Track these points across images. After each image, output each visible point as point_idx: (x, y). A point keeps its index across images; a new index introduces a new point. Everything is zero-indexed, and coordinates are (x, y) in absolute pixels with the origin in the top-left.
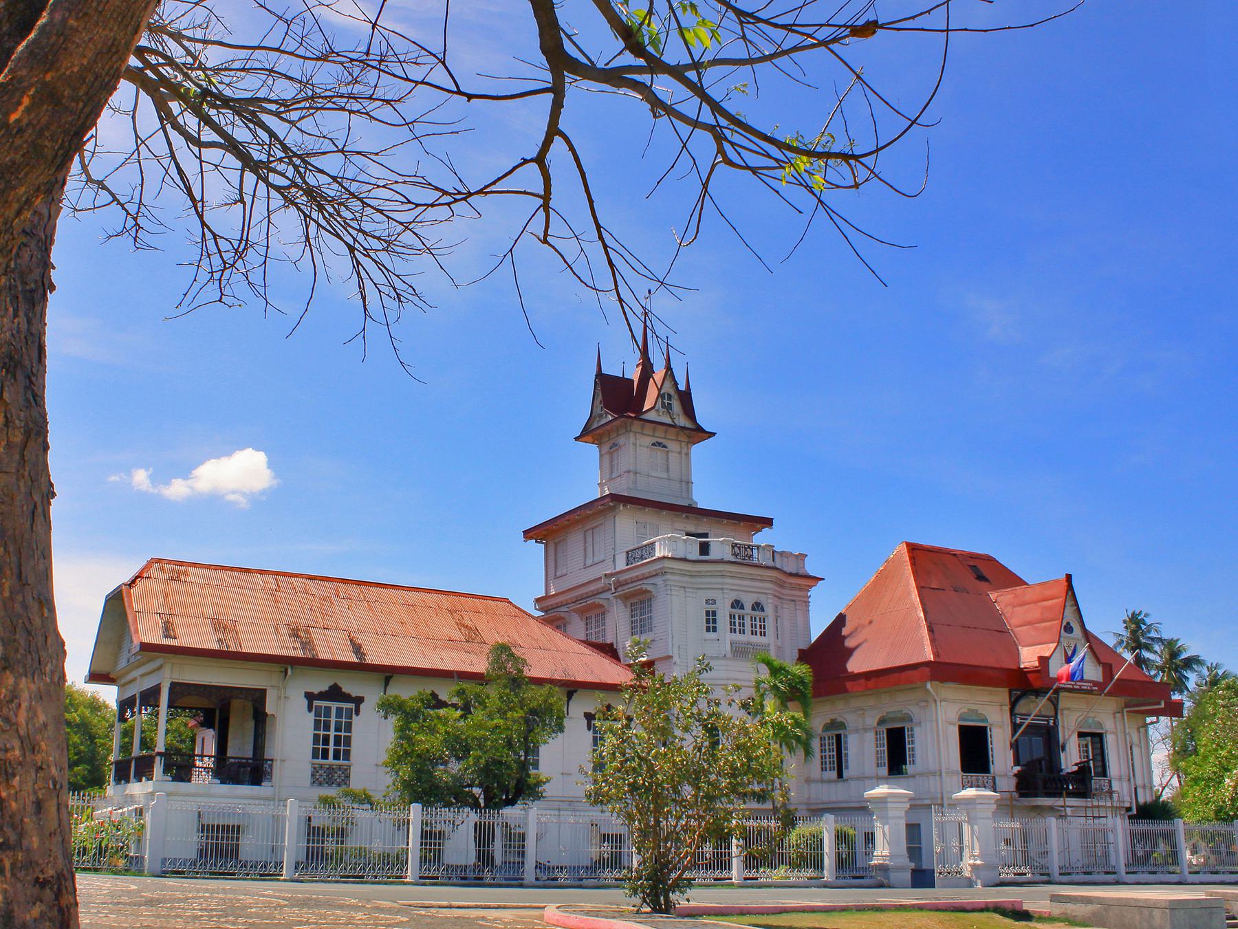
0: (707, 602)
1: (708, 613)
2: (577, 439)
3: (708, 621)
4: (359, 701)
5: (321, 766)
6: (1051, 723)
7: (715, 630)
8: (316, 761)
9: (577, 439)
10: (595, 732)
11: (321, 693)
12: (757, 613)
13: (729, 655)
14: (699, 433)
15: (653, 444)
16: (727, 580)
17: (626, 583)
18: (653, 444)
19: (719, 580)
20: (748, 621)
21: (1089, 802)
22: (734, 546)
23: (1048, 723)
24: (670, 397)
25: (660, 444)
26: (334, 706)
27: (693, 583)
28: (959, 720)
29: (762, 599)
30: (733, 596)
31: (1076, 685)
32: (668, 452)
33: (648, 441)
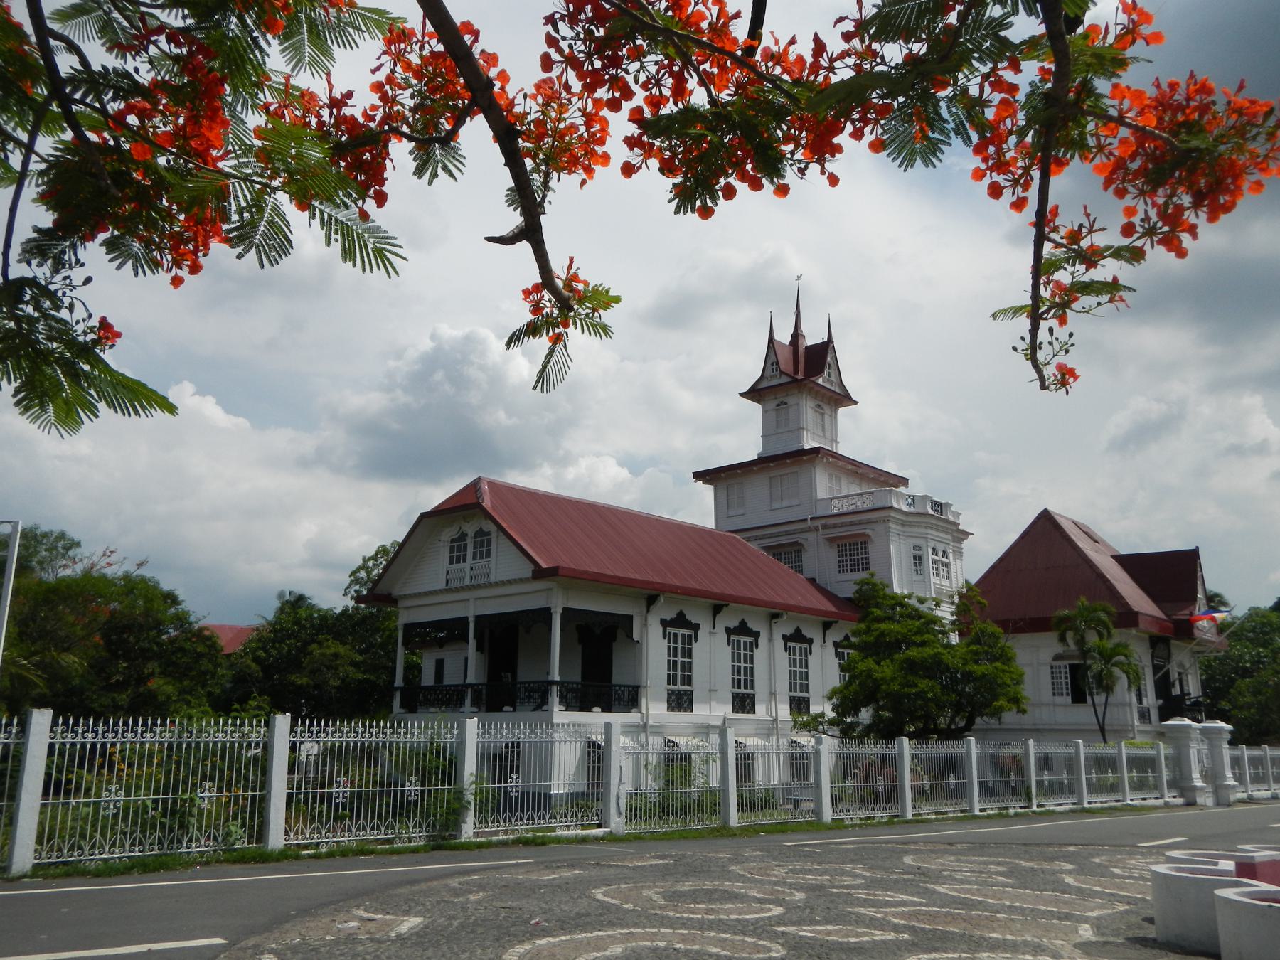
1: (915, 558)
2: (742, 395)
4: (696, 627)
5: (673, 691)
8: (672, 687)
9: (742, 395)
11: (672, 620)
12: (945, 560)
14: (844, 398)
16: (929, 531)
17: (834, 526)
19: (922, 530)
20: (941, 568)
25: (818, 406)
26: (680, 632)
30: (932, 544)
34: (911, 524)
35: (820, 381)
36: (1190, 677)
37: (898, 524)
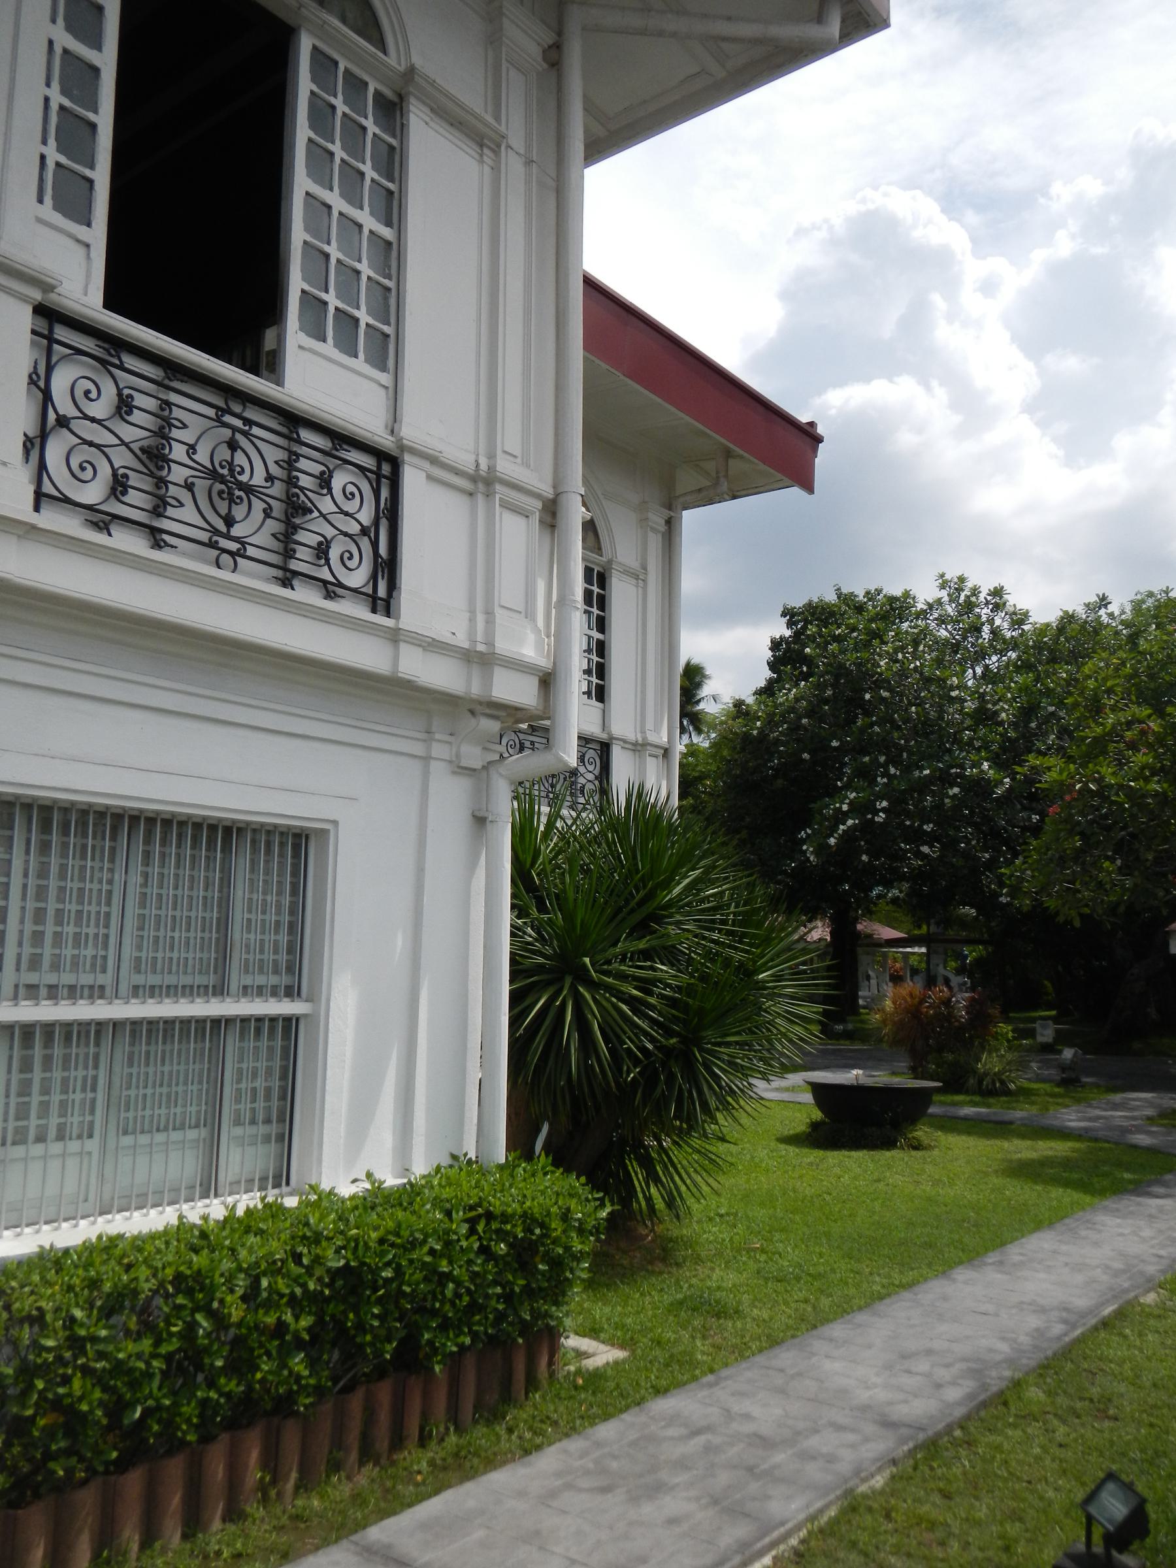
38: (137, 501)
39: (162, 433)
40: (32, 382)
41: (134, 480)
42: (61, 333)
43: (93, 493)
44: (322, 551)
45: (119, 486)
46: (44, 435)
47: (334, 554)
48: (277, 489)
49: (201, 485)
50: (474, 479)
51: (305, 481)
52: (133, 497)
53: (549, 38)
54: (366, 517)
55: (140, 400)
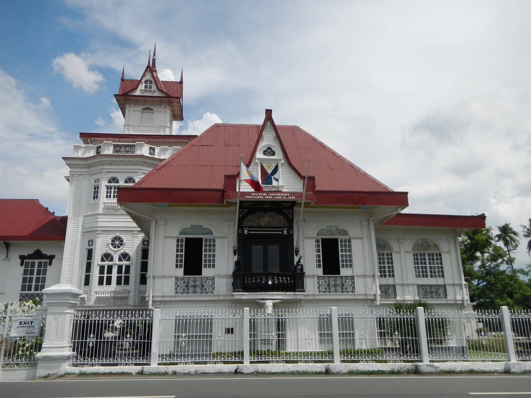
0: (95, 182)
1: (95, 188)
3: (95, 192)
6: (285, 232)
7: (97, 198)
10: (27, 265)
13: (100, 211)
15: (144, 109)
18: (144, 109)
19: (101, 167)
21: (299, 295)
22: (115, 146)
23: (283, 232)
24: (151, 82)
25: (148, 109)
27: (88, 172)
28: (180, 234)
29: (132, 175)
30: (111, 175)
31: (268, 195)
32: (153, 113)
33: (140, 108)
34: (94, 165)
35: (137, 93)
36: (356, 245)
37: (82, 168)
38: (327, 290)
39: (329, 283)
40: (318, 283)
41: (327, 288)
42: (320, 278)
43: (324, 290)
44: (346, 288)
45: (326, 289)
46: (319, 287)
47: (347, 288)
48: (341, 284)
49: (333, 287)
50: (363, 276)
51: (343, 282)
52: (327, 289)
53: (368, 222)
54: (351, 284)
55: (327, 281)
